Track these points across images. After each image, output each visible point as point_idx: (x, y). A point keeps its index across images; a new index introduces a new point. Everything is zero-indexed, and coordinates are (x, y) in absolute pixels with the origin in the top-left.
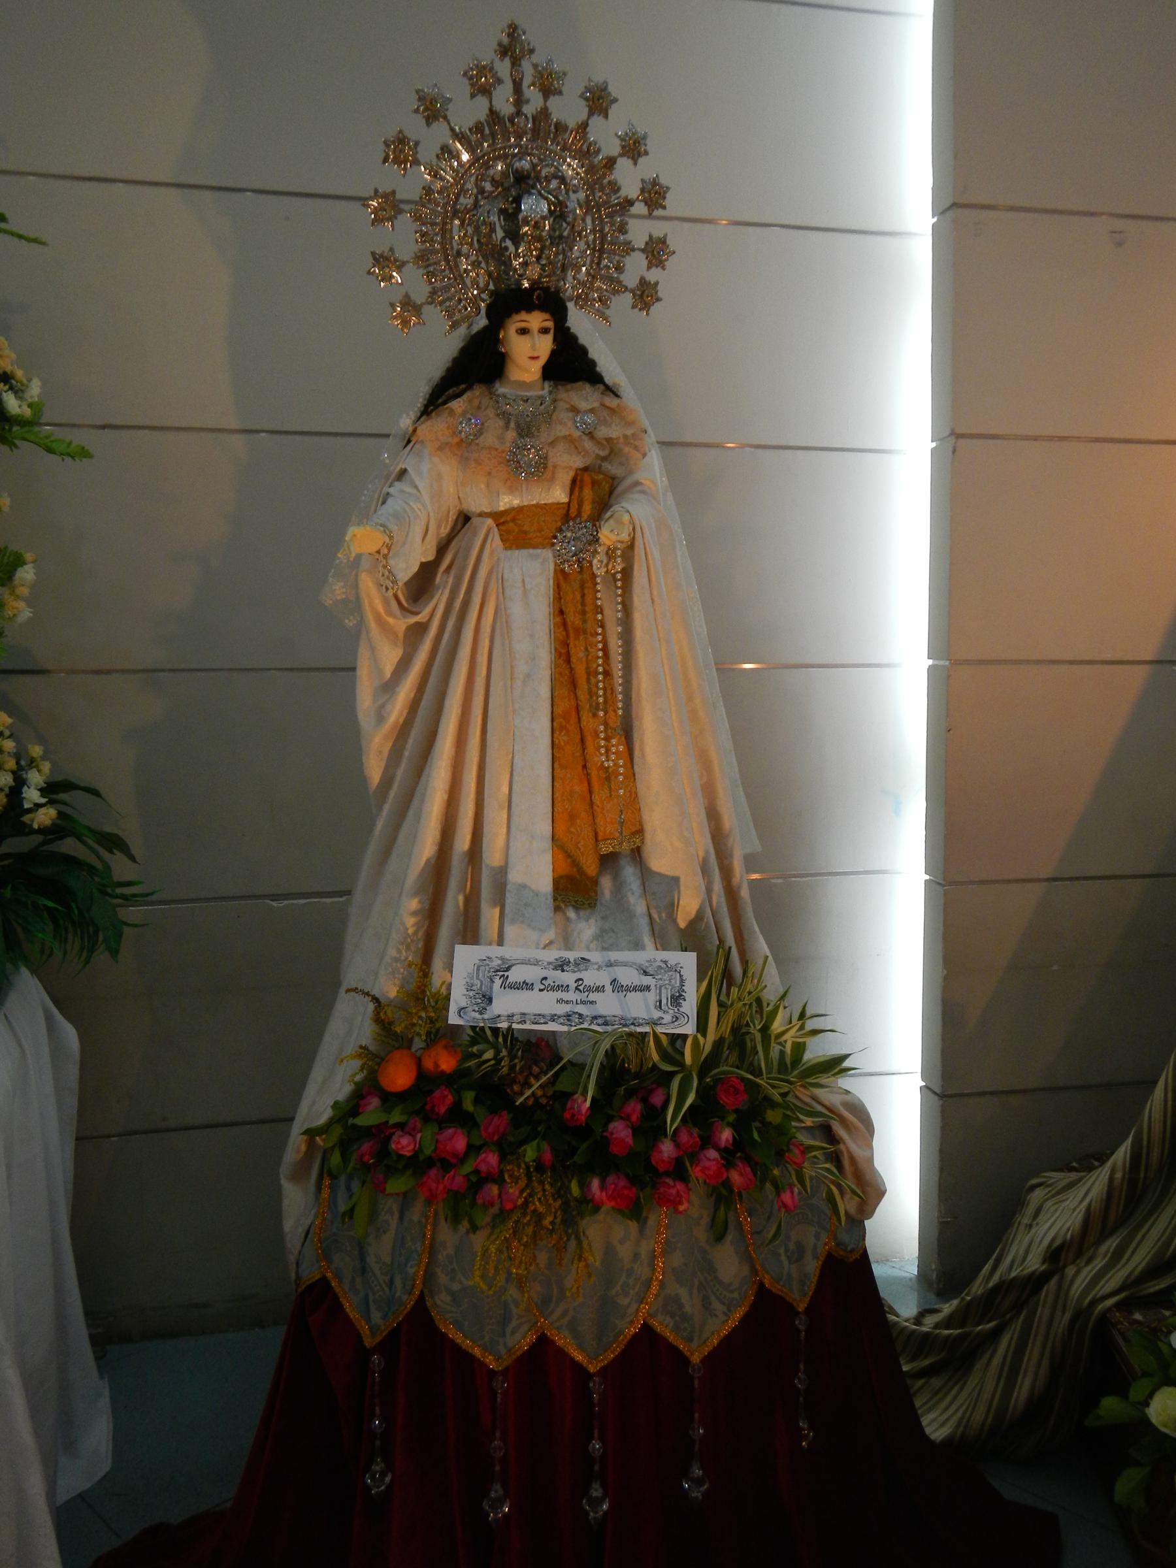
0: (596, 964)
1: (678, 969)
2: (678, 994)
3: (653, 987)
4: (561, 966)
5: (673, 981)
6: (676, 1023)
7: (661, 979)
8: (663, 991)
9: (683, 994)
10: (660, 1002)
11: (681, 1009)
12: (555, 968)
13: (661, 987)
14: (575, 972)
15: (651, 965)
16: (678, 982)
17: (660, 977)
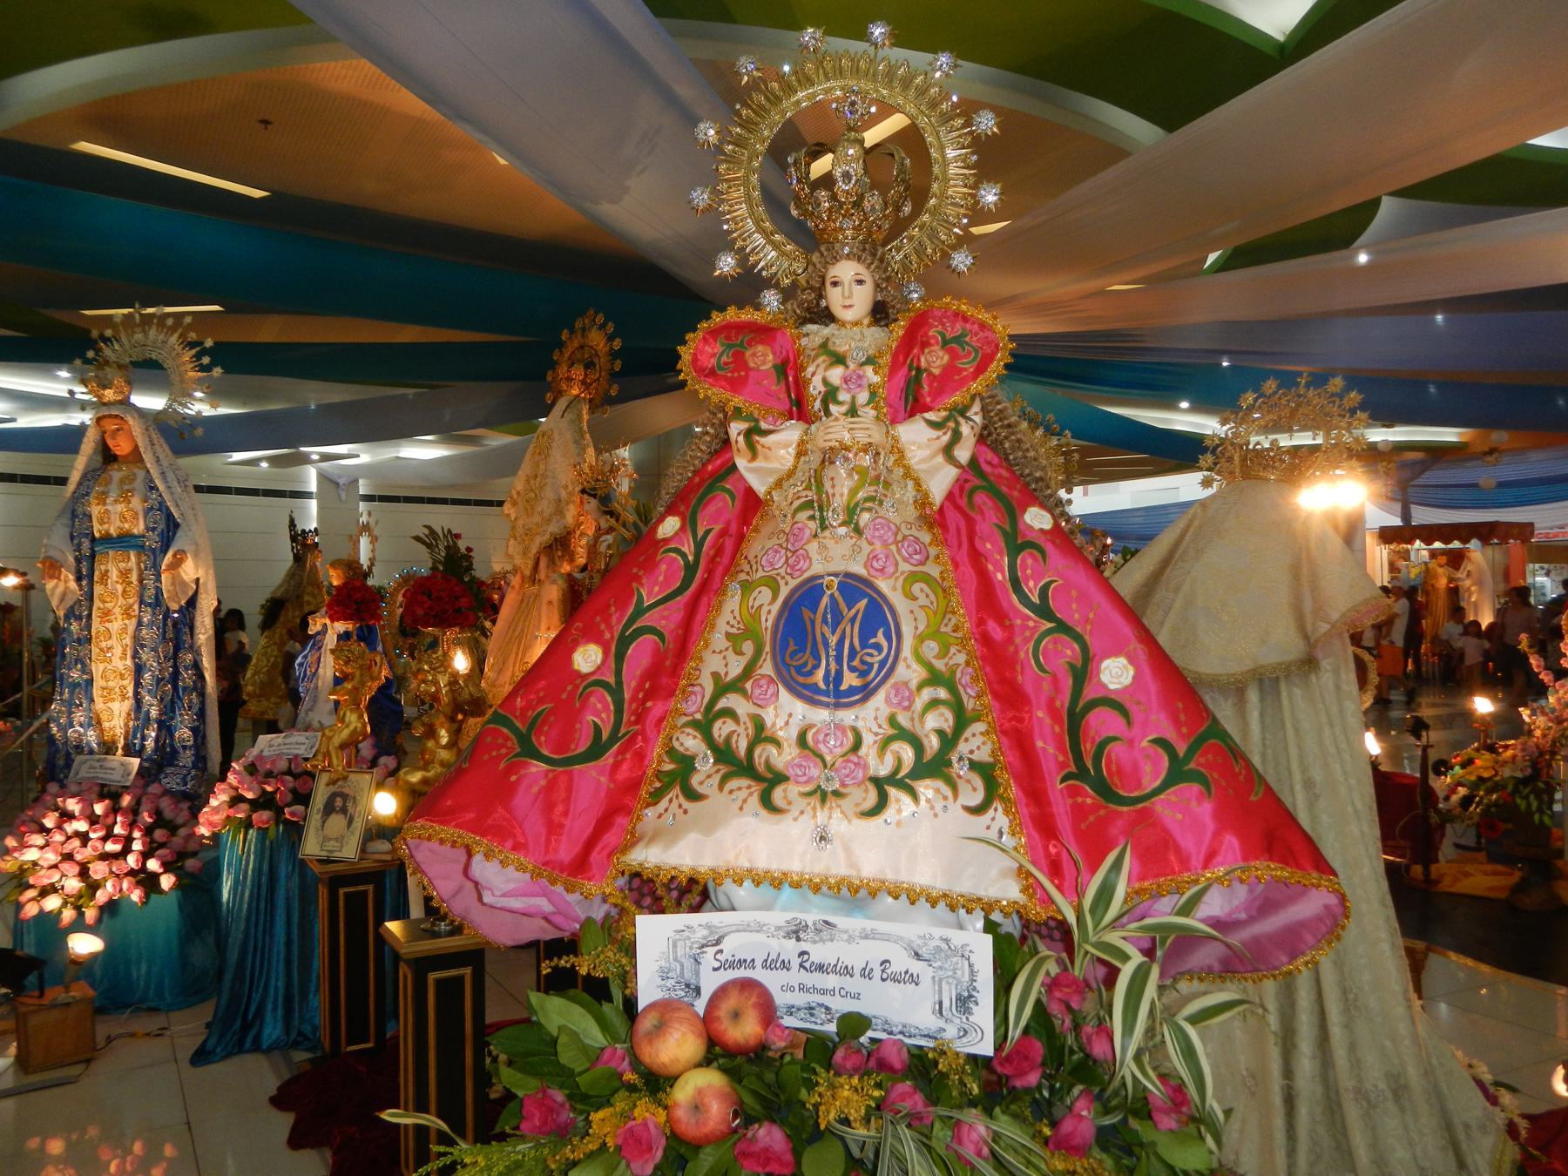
0: (846, 932)
1: (966, 954)
2: (966, 994)
3: (926, 981)
4: (796, 932)
5: (959, 972)
6: (964, 1040)
7: (941, 968)
8: (945, 986)
9: (974, 993)
10: (941, 1003)
11: (971, 1018)
12: (788, 936)
13: (941, 981)
14: (815, 942)
15: (926, 944)
16: (966, 978)
17: (939, 963)
